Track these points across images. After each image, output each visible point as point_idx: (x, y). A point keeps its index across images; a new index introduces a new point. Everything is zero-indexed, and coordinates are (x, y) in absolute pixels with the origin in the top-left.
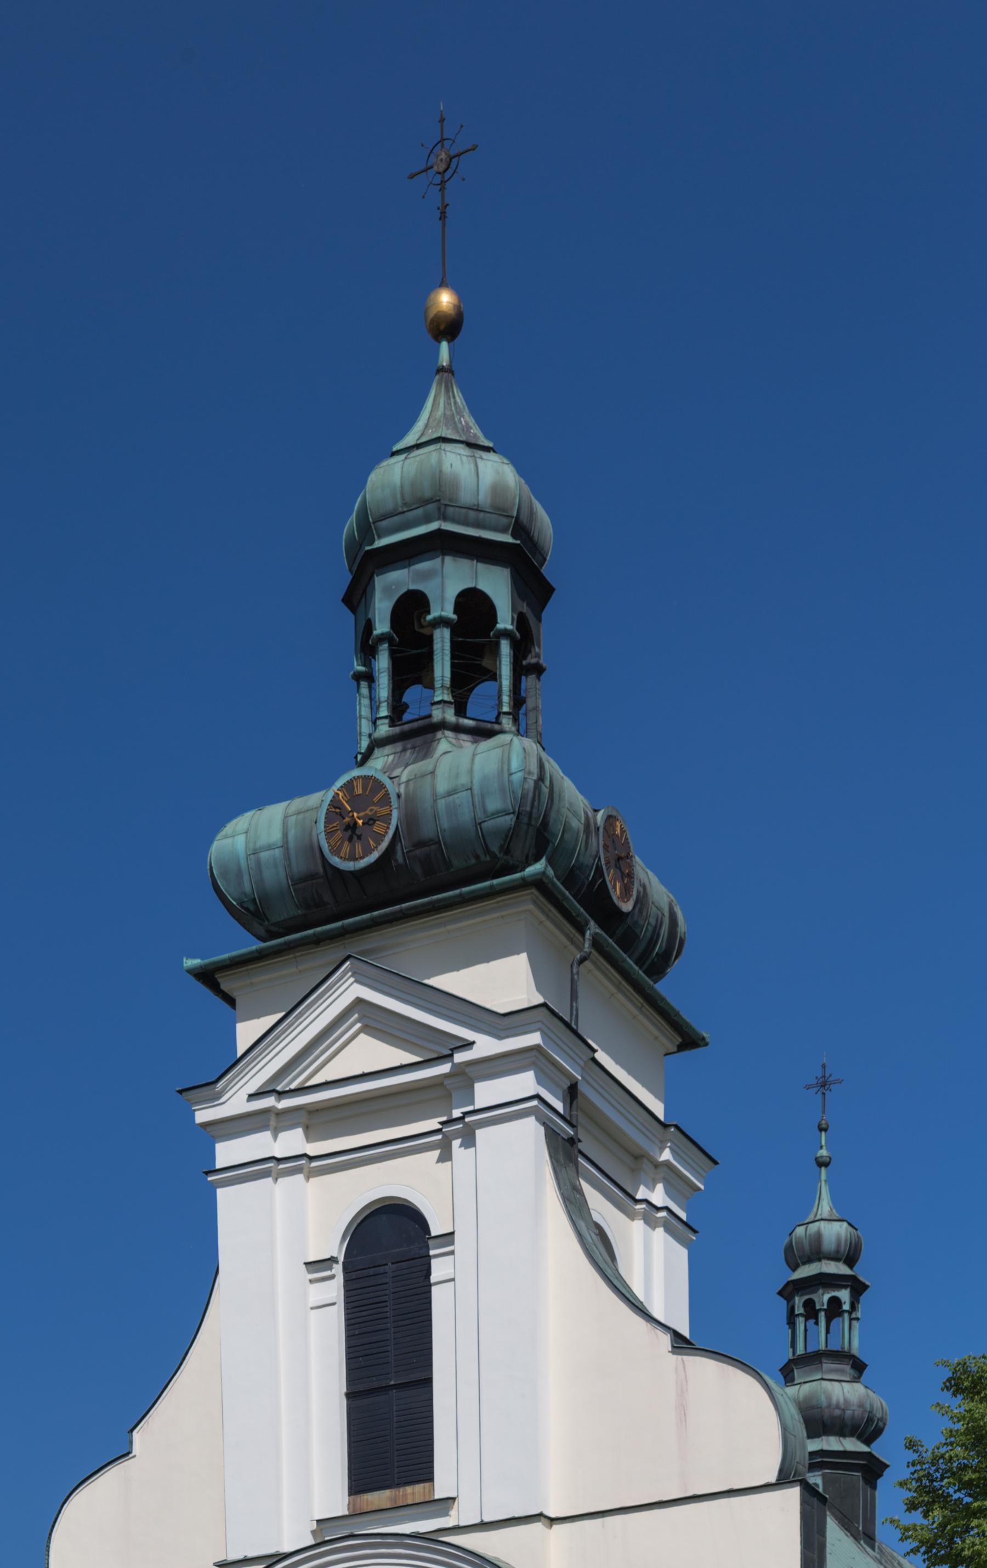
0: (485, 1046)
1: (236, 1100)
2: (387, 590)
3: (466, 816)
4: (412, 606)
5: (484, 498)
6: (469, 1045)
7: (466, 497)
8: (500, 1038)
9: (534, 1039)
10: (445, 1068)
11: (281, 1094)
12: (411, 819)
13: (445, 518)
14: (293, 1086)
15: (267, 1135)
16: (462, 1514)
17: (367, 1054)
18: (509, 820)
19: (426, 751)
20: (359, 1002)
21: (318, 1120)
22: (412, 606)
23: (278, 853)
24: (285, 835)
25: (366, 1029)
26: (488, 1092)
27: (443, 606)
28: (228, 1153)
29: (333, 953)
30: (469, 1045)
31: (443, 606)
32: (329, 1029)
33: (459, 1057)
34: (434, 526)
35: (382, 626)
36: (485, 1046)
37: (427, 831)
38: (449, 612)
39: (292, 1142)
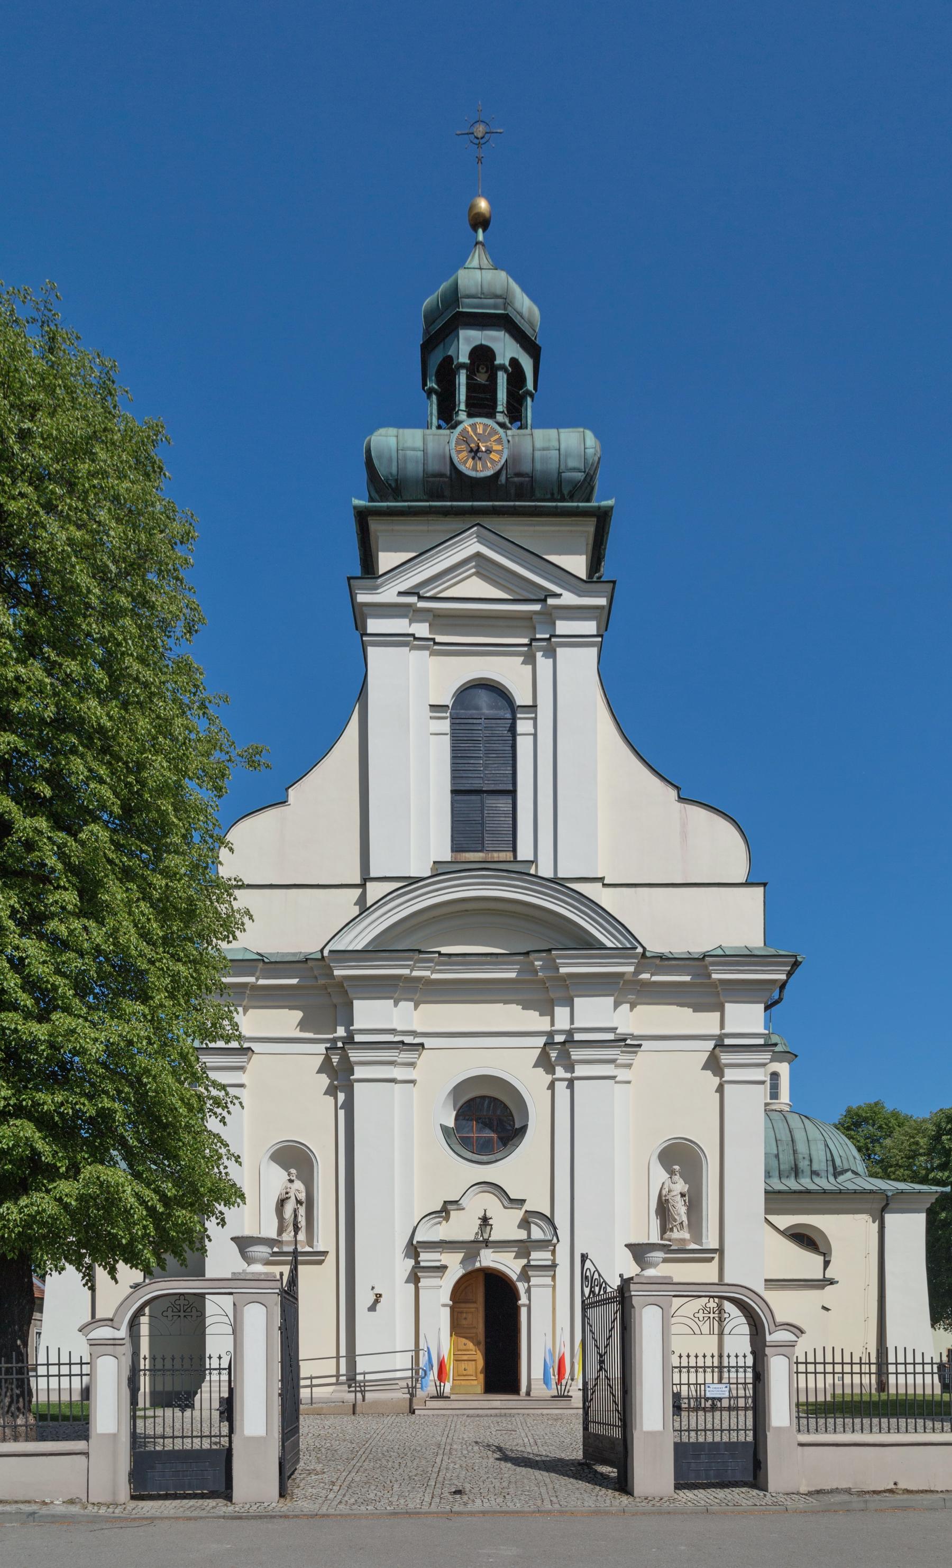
0: (568, 598)
1: (388, 594)
2: (468, 340)
6: (559, 596)
8: (580, 596)
10: (537, 607)
11: (421, 598)
14: (428, 595)
15: (407, 621)
17: (476, 587)
18: (580, 476)
20: (478, 555)
21: (440, 620)
25: (477, 574)
26: (563, 627)
28: (374, 625)
30: (559, 596)
32: (458, 565)
33: (551, 601)
35: (464, 358)
36: (568, 598)
39: (422, 629)
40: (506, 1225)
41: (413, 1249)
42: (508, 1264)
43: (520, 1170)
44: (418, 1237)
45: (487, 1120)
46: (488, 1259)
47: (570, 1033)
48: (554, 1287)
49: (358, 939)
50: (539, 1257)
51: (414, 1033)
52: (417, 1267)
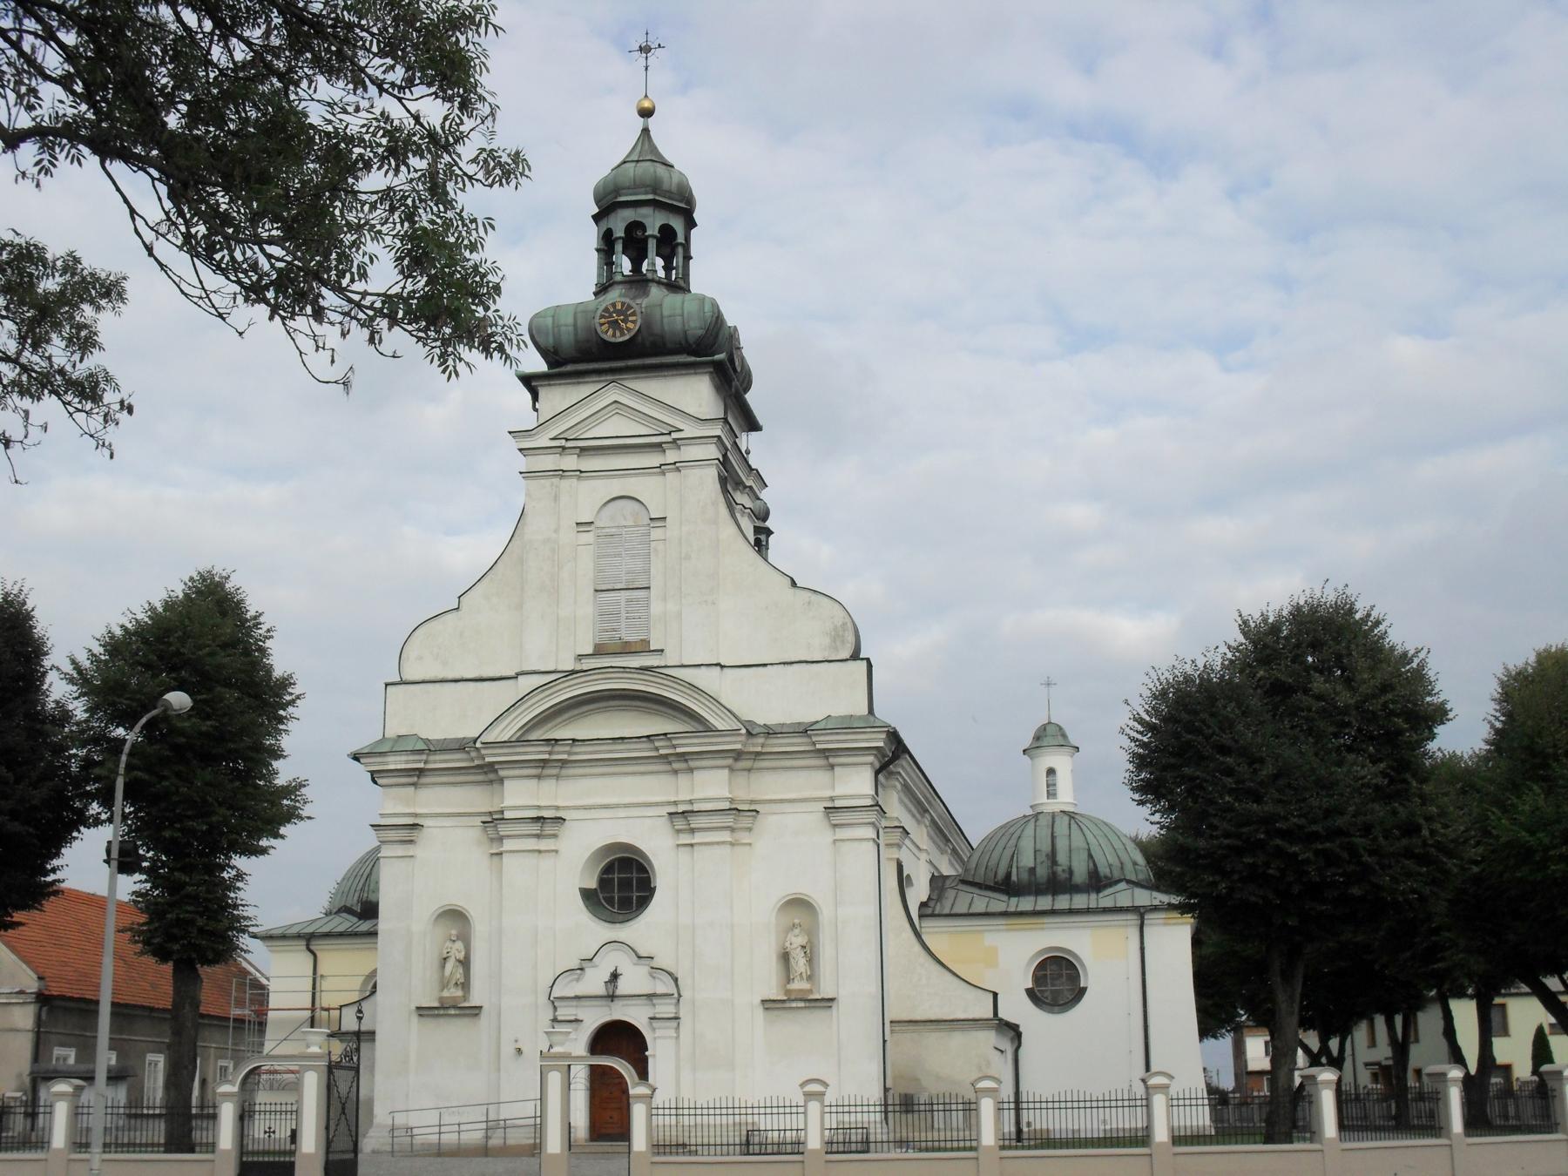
3: (678, 326)
4: (635, 227)
5: (674, 188)
7: (666, 186)
9: (718, 432)
12: (647, 324)
13: (655, 193)
16: (671, 658)
19: (646, 293)
22: (635, 227)
23: (571, 329)
24: (575, 319)
27: (653, 229)
29: (610, 378)
31: (653, 229)
33: (674, 435)
34: (650, 197)
36: (690, 430)
37: (657, 329)
38: (656, 233)
40: (634, 980)
41: (554, 1003)
42: (636, 1015)
43: (646, 929)
44: (556, 993)
45: (622, 885)
46: (620, 1012)
47: (691, 802)
48: (677, 1038)
49: (505, 731)
50: (665, 1009)
51: (557, 808)
52: (555, 1020)
